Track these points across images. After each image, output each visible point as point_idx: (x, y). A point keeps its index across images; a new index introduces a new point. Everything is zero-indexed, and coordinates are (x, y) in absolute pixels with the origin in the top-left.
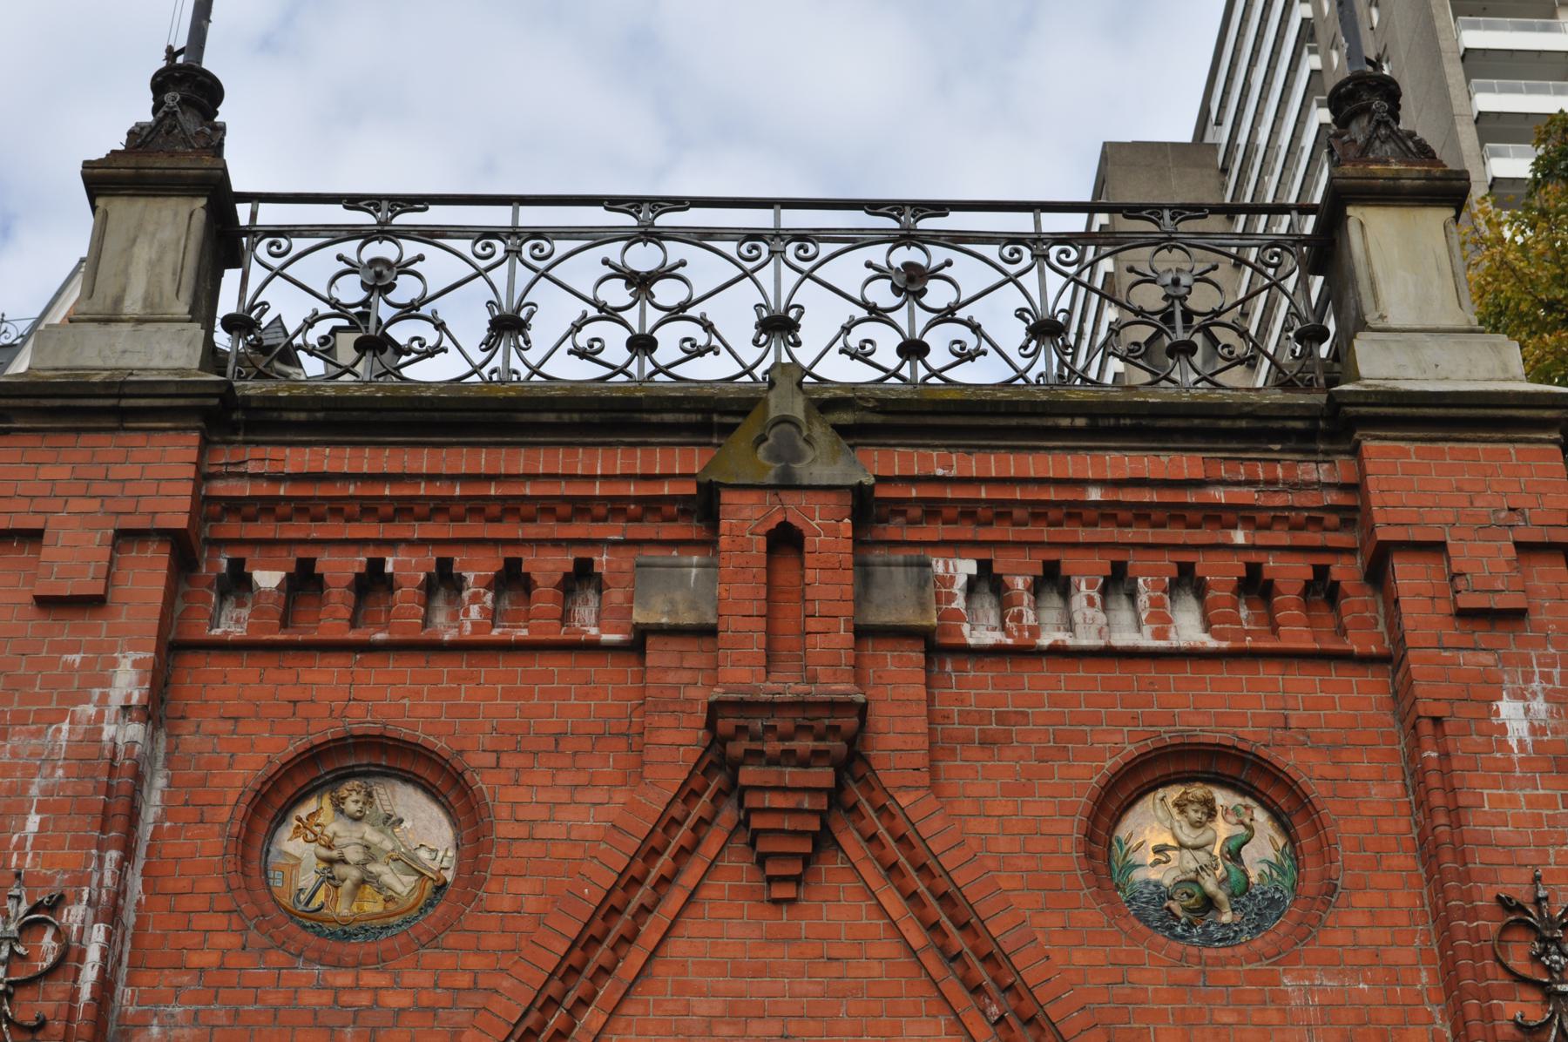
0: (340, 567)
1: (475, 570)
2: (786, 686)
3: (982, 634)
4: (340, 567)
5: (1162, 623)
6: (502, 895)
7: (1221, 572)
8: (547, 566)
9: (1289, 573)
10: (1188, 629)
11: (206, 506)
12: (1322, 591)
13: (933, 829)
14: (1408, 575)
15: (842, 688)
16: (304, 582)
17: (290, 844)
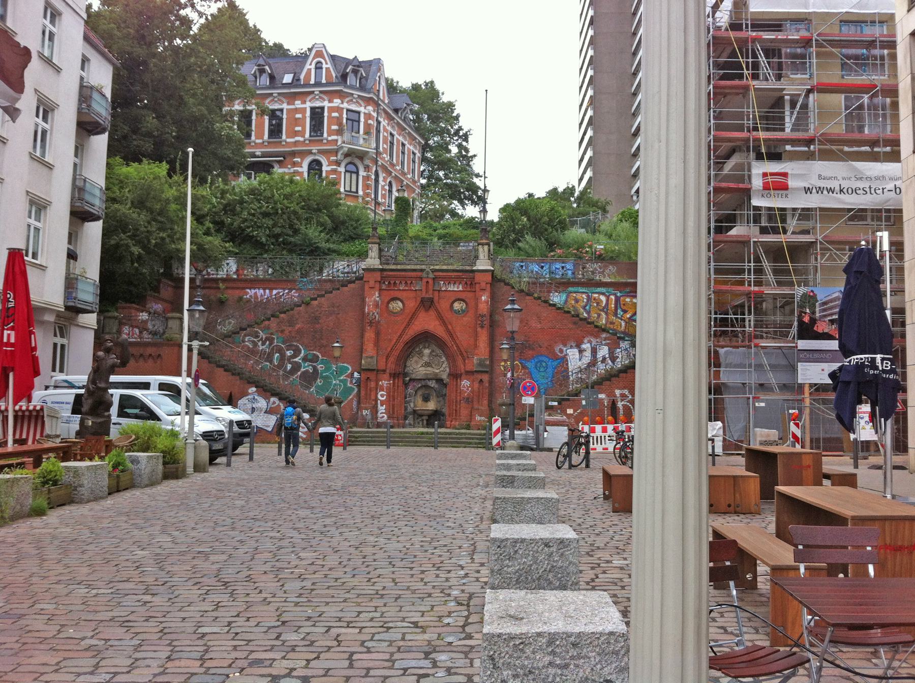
0: (392, 282)
1: (403, 282)
2: (427, 296)
3: (444, 289)
4: (392, 282)
5: (458, 288)
6: (407, 311)
7: (463, 283)
8: (409, 282)
9: (469, 283)
10: (461, 288)
11: (382, 277)
12: (471, 284)
13: (438, 307)
14: (477, 285)
15: (431, 296)
16: (389, 283)
17: (390, 305)
